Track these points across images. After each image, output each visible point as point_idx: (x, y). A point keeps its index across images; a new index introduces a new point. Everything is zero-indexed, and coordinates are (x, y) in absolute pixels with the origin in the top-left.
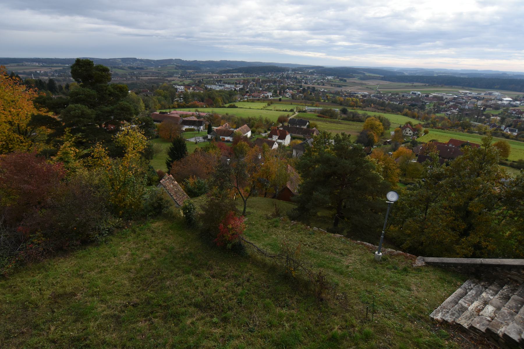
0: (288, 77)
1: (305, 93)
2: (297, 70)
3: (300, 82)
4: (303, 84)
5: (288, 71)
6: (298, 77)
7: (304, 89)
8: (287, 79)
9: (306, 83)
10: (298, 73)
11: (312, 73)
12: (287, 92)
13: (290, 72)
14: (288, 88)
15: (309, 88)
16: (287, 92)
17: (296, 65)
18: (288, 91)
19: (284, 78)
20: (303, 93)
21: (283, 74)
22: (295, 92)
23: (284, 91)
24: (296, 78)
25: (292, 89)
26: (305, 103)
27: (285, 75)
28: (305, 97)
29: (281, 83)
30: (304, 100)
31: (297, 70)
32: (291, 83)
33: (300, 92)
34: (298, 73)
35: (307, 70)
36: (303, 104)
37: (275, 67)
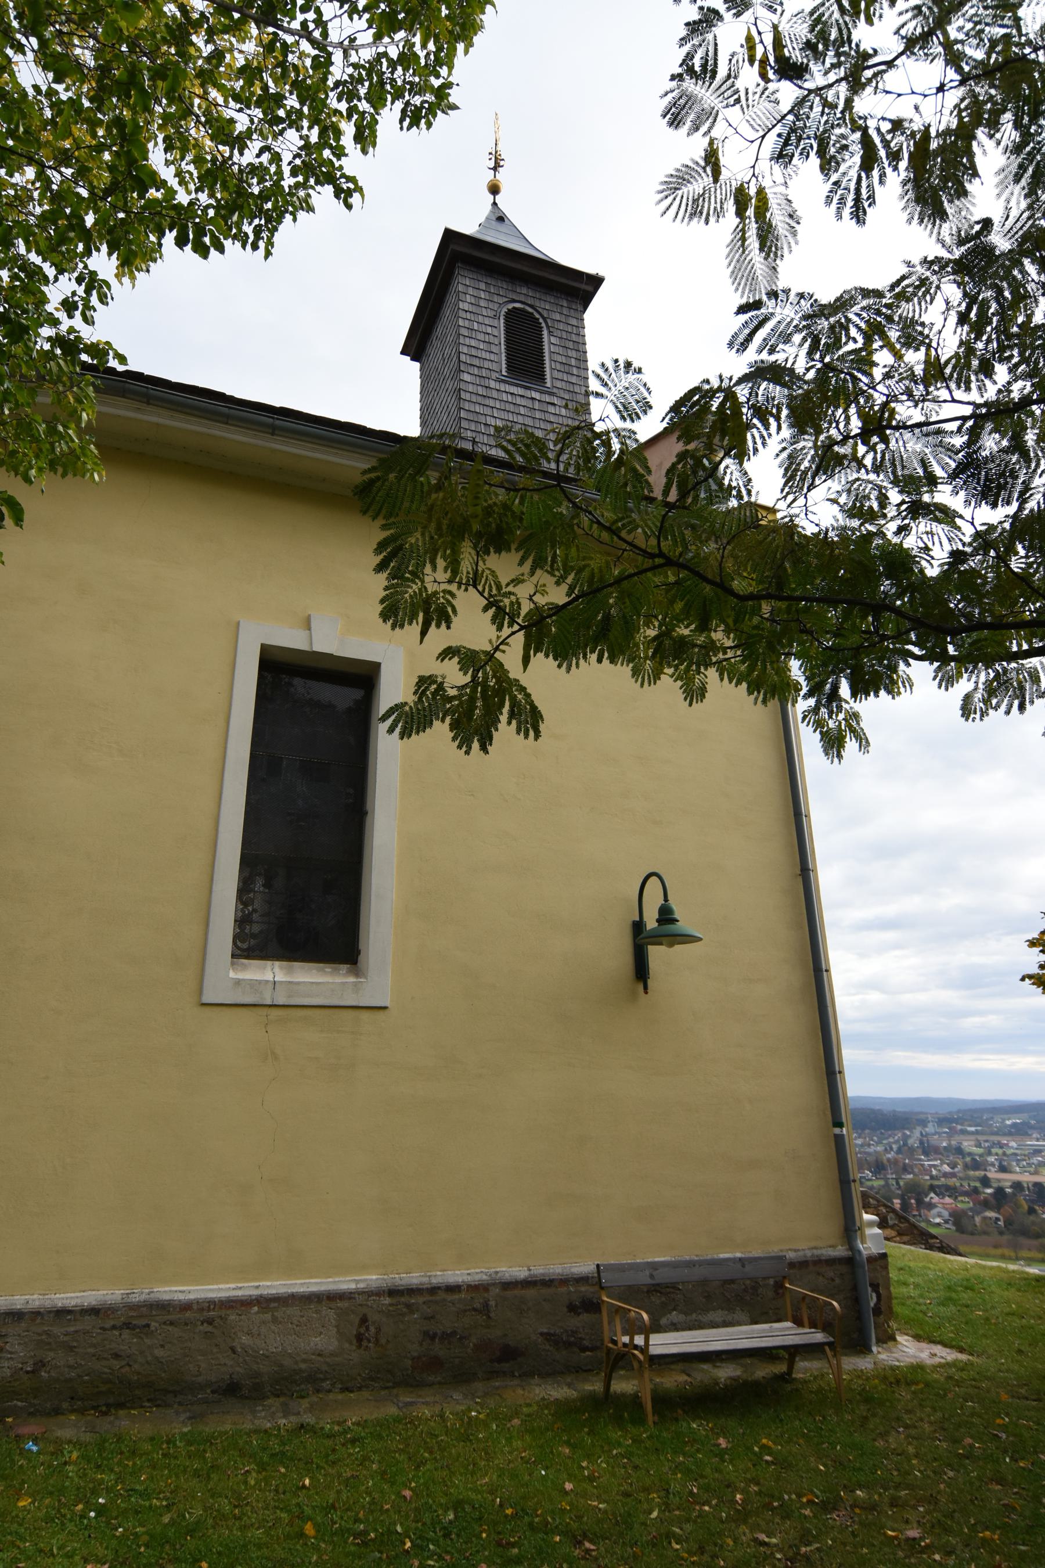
0: (928, 1150)
1: (1007, 1209)
2: (957, 1121)
3: (976, 1165)
4: (992, 1174)
5: (923, 1123)
6: (968, 1145)
7: (1000, 1192)
8: (926, 1153)
9: (1003, 1169)
10: (963, 1132)
11: (1020, 1131)
12: (931, 1206)
13: (930, 1128)
14: (932, 1188)
15: (1017, 1186)
16: (931, 1206)
17: (950, 1101)
18: (936, 1199)
19: (912, 1150)
20: (998, 1208)
21: (906, 1138)
22: (965, 1204)
23: (920, 1202)
24: (959, 1151)
25: (952, 1192)
26: (1015, 1247)
27: (913, 1142)
28: (1008, 1222)
29: (906, 1169)
30: (1005, 1237)
31: (957, 1121)
32: (946, 1168)
33: (986, 1204)
34: (963, 1132)
35: (998, 1118)
36: (1007, 1252)
37: (873, 1111)
